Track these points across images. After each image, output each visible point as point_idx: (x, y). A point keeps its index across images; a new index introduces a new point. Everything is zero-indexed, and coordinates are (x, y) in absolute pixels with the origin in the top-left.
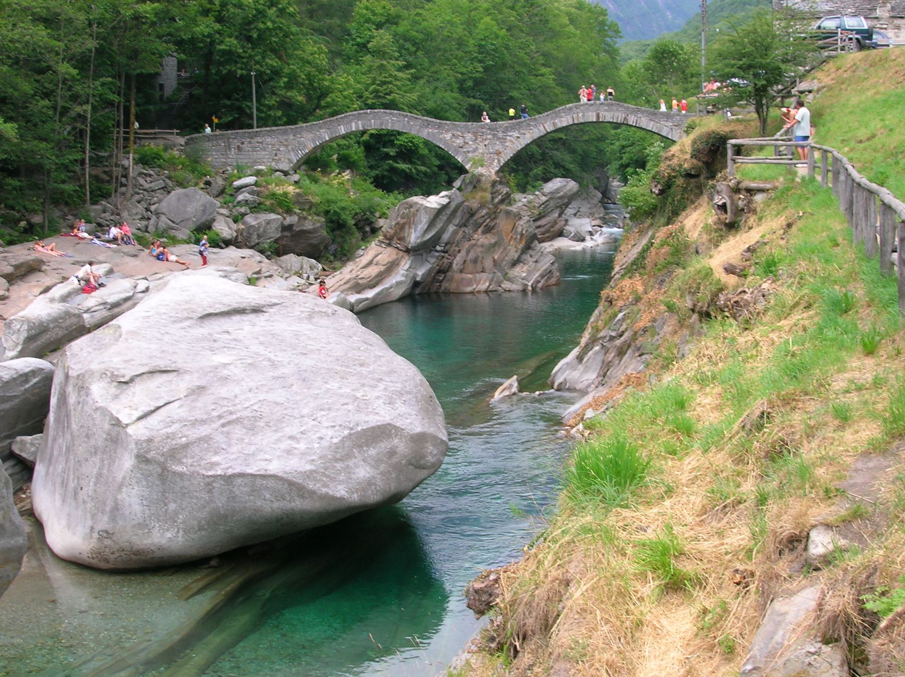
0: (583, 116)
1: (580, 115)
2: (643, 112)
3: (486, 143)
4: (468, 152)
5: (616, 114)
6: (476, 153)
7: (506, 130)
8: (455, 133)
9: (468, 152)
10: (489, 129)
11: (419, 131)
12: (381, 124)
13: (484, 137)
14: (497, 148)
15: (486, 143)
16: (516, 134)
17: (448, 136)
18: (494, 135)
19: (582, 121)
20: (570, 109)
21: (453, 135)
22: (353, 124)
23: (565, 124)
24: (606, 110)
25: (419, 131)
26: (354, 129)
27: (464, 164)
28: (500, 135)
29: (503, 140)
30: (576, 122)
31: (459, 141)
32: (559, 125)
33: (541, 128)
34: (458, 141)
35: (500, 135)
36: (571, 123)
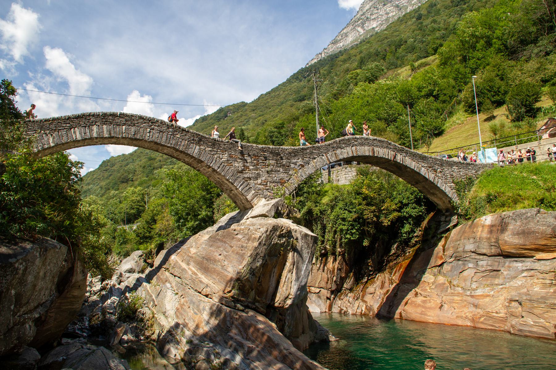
4: (250, 179)
6: (259, 181)
9: (250, 179)
10: (271, 153)
14: (282, 175)
16: (300, 162)
17: (225, 157)
19: (360, 154)
21: (230, 156)
23: (345, 156)
24: (377, 146)
25: (188, 146)
29: (287, 168)
30: (355, 155)
31: (239, 165)
32: (341, 157)
35: (284, 162)
36: (351, 155)
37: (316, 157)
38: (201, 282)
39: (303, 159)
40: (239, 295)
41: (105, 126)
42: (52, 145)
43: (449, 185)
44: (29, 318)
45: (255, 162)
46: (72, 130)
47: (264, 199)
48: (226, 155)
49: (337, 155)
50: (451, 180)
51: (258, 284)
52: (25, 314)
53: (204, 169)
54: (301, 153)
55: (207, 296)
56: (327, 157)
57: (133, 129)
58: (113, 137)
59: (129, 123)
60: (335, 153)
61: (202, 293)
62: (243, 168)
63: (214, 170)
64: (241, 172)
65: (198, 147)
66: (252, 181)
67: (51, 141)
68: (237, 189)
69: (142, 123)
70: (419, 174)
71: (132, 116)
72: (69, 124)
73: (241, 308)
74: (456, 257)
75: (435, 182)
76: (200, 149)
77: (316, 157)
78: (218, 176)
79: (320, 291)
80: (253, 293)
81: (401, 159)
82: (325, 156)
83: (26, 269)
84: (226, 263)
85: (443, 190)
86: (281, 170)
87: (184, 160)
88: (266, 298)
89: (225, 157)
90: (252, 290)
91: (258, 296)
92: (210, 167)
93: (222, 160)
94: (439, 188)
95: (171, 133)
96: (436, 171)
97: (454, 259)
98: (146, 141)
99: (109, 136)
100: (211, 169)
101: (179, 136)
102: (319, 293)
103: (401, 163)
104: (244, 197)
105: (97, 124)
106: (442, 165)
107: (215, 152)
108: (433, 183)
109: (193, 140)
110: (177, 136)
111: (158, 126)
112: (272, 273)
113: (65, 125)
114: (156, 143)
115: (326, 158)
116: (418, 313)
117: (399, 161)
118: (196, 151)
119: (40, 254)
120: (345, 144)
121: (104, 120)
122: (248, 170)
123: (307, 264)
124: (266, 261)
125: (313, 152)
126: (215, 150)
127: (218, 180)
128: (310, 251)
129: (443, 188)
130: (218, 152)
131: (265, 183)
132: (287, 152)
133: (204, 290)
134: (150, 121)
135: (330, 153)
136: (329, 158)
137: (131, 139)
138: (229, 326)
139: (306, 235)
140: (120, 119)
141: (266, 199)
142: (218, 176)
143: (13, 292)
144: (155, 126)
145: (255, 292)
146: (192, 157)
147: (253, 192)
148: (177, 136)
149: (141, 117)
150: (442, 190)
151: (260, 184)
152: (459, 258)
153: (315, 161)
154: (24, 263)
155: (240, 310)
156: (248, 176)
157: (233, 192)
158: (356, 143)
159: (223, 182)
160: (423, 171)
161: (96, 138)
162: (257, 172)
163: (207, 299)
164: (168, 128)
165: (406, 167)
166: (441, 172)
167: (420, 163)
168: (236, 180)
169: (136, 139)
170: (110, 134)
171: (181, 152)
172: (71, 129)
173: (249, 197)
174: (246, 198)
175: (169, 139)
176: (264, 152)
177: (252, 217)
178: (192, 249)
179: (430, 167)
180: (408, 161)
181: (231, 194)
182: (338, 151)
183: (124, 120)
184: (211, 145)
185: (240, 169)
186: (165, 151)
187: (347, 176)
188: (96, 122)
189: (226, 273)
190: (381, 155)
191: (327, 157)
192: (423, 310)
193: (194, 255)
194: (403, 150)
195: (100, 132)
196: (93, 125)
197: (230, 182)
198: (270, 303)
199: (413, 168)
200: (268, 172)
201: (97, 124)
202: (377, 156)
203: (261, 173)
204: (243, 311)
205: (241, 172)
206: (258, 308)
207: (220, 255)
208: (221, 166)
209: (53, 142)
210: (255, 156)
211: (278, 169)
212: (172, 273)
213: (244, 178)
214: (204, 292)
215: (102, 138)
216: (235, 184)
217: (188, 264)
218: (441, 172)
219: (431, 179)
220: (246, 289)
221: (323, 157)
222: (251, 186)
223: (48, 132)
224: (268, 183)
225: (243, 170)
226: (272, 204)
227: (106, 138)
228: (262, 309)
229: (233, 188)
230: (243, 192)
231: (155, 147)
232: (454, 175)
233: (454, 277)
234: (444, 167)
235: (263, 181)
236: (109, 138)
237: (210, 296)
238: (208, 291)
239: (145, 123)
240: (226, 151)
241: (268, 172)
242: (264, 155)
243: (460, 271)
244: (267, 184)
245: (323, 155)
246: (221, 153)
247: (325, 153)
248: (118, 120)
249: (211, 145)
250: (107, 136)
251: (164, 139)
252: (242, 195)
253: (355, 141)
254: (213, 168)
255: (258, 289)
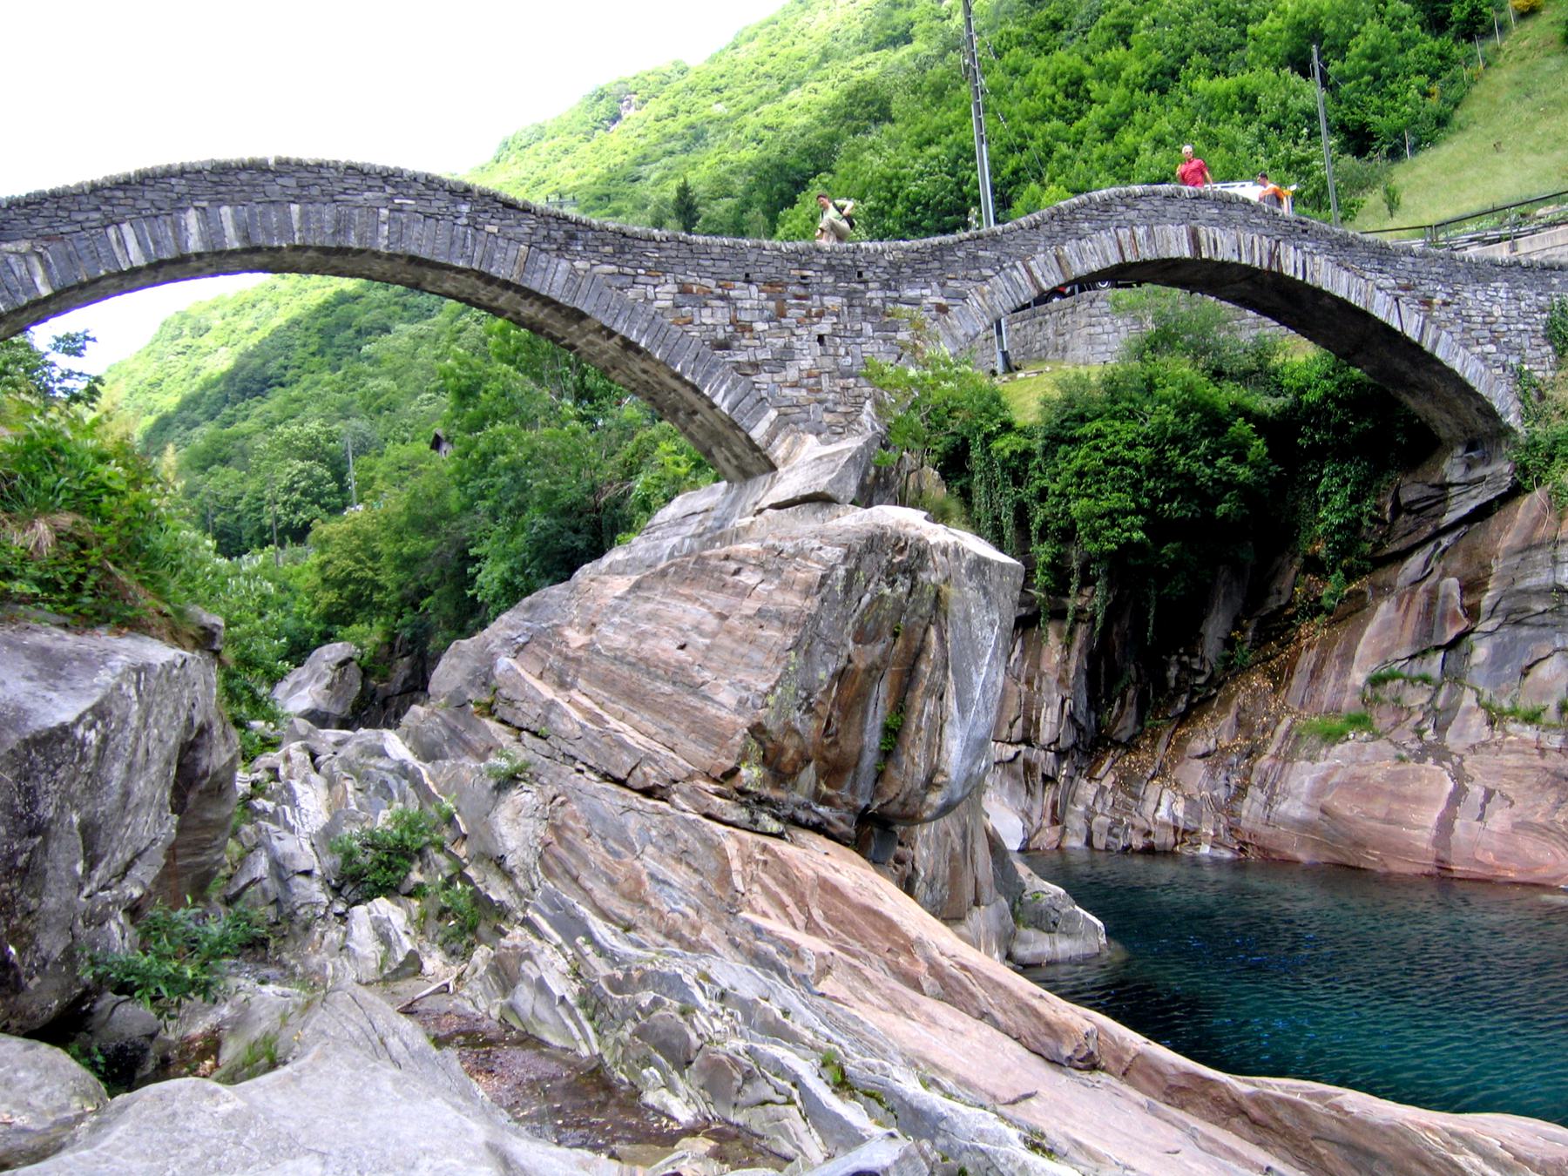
0: (1150, 236)
1: (1141, 232)
2: (1318, 236)
3: (825, 327)
5: (1246, 236)
6: (792, 374)
7: (894, 276)
8: (692, 278)
9: (756, 366)
10: (830, 268)
11: (527, 265)
12: (341, 227)
13: (814, 303)
15: (825, 327)
16: (932, 296)
17: (664, 295)
18: (850, 295)
19: (1148, 254)
20: (1107, 204)
21: (684, 290)
22: (191, 219)
23: (1094, 265)
24: (1212, 221)
25: (527, 265)
26: (194, 244)
27: (745, 423)
28: (875, 295)
30: (1130, 258)
31: (714, 318)
32: (1078, 269)
33: (1020, 275)
34: (706, 317)
36: (1114, 260)
37: (990, 273)
38: (623, 745)
39: (942, 285)
40: (763, 782)
41: (226, 211)
42: (45, 291)
43: (1478, 349)
44: (115, 902)
45: (772, 304)
46: (111, 231)
47: (811, 439)
48: (668, 288)
49: (1063, 263)
50: (1487, 333)
51: (827, 741)
52: (103, 888)
53: (591, 343)
54: (936, 264)
55: (648, 792)
56: (1029, 271)
57: (328, 213)
58: (257, 250)
59: (315, 191)
60: (1058, 258)
61: (630, 782)
62: (730, 329)
63: (628, 345)
64: (724, 345)
65: (564, 265)
66: (764, 378)
67: (38, 280)
68: (713, 406)
69: (358, 190)
70: (1364, 316)
71: (320, 165)
72: (98, 209)
73: (775, 827)
74: (1508, 613)
75: (1427, 346)
76: (574, 271)
77: (990, 273)
78: (644, 365)
79: (1018, 754)
80: (808, 775)
81: (1300, 265)
82: (1023, 271)
83: (105, 740)
84: (707, 675)
85: (1457, 369)
86: (868, 328)
87: (518, 313)
88: (853, 790)
89: (664, 295)
90: (809, 761)
91: (828, 785)
92: (611, 334)
93: (657, 304)
94: (1439, 362)
95: (464, 221)
96: (1427, 302)
97: (1500, 620)
98: (376, 255)
99: (246, 245)
100: (616, 339)
101: (495, 229)
102: (1012, 761)
103: (1300, 277)
104: (742, 435)
105: (197, 204)
106: (1446, 279)
107: (630, 280)
108: (1417, 347)
109: (547, 238)
110: (489, 228)
111: (419, 197)
112: (872, 702)
113: (81, 217)
114: (414, 260)
115: (1026, 276)
116: (1373, 818)
117: (1290, 272)
118: (560, 279)
119: (138, 690)
120: (1088, 219)
121: (223, 189)
122: (747, 335)
123: (989, 665)
124: (850, 660)
125: (976, 258)
126: (627, 270)
127: (645, 377)
128: (996, 616)
129: (1456, 365)
130: (640, 279)
131: (812, 381)
132: (883, 263)
133: (637, 772)
134: (386, 179)
135: (1040, 258)
136: (1038, 274)
137: (325, 251)
138: (741, 888)
139: (980, 564)
140: (280, 181)
141: (818, 434)
142: (644, 365)
143: (76, 819)
144: (407, 197)
145: (817, 768)
146: (548, 302)
147: (773, 414)
148: (489, 228)
149: (352, 169)
150: (1451, 371)
151: (795, 385)
152: (1520, 617)
153: (987, 288)
154: (99, 725)
155: (771, 835)
156: (753, 359)
157: (699, 417)
158: (1132, 214)
159: (661, 384)
160: (1381, 309)
161: (199, 256)
162: (780, 343)
163: (651, 802)
164: (456, 204)
165: (1318, 293)
166: (1445, 304)
167: (1368, 275)
168: (709, 374)
169: (343, 251)
170: (247, 237)
171: (507, 285)
172: (106, 227)
173: (758, 433)
174: (749, 439)
175: (459, 243)
176: (803, 267)
177: (778, 506)
178: (570, 633)
179: (1406, 289)
180: (1323, 269)
181: (692, 428)
182: (1068, 249)
183: (291, 182)
184: (613, 255)
185: (721, 335)
186: (448, 286)
187: (1099, 329)
188: (194, 197)
189: (712, 710)
190: (1226, 254)
191: (1029, 271)
192: (1396, 806)
193: (581, 653)
194: (1305, 231)
195: (212, 229)
196: (185, 210)
197: (686, 383)
198: (867, 807)
199: (1341, 293)
200: (821, 339)
201: (197, 204)
202: (1209, 261)
203: (798, 345)
204: (779, 836)
205: (724, 345)
206: (829, 823)
207: (682, 647)
208: (655, 328)
209: (49, 279)
210: (771, 285)
211: (858, 327)
212: (507, 718)
213: (737, 367)
214: (637, 780)
215: (220, 253)
216: (706, 391)
217: (563, 685)
218: (1445, 304)
219: (1412, 333)
220: (785, 759)
221: (1015, 273)
222: (764, 394)
223: (24, 246)
224: (825, 380)
225: (733, 338)
226: (848, 455)
227: (233, 252)
228: (843, 827)
229: (701, 405)
230: (735, 416)
231: (410, 273)
232: (1497, 311)
233: (1504, 686)
234: (1457, 287)
235: (804, 374)
236: (245, 251)
237: (659, 792)
238: (651, 774)
239: (370, 188)
240: (664, 273)
241: (821, 339)
242: (804, 277)
243: (1526, 662)
244: (819, 383)
245: (1014, 267)
246: (649, 280)
247: (1023, 259)
248: (274, 190)
249: (613, 255)
250: (237, 245)
251: (442, 242)
252: (734, 426)
253: (1127, 206)
254: (623, 338)
255: (825, 759)
